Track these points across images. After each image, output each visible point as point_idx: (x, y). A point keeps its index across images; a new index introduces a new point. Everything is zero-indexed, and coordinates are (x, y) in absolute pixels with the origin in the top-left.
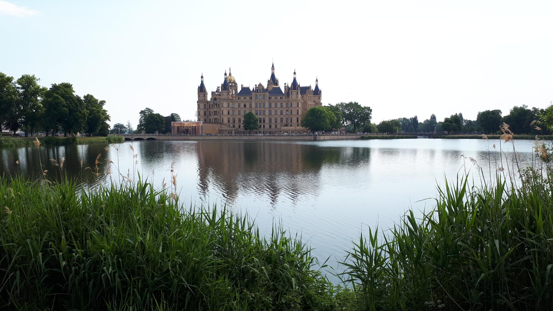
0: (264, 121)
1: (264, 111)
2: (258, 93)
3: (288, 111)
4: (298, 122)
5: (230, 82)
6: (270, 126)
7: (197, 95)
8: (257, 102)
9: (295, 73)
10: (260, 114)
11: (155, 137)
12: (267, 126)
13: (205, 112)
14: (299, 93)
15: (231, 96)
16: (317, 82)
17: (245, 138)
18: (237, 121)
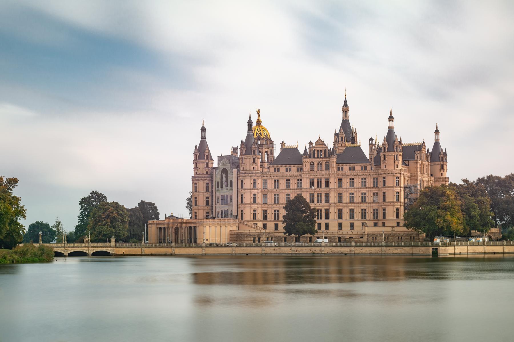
0: (327, 216)
1: (327, 196)
2: (314, 160)
3: (377, 193)
4: (397, 216)
5: (259, 139)
6: (340, 226)
7: (192, 166)
8: (312, 177)
9: (391, 118)
10: (319, 201)
11: (110, 249)
12: (333, 226)
13: (207, 198)
14: (400, 158)
15: (261, 166)
16: (439, 135)
17: (287, 250)
18: (271, 216)
